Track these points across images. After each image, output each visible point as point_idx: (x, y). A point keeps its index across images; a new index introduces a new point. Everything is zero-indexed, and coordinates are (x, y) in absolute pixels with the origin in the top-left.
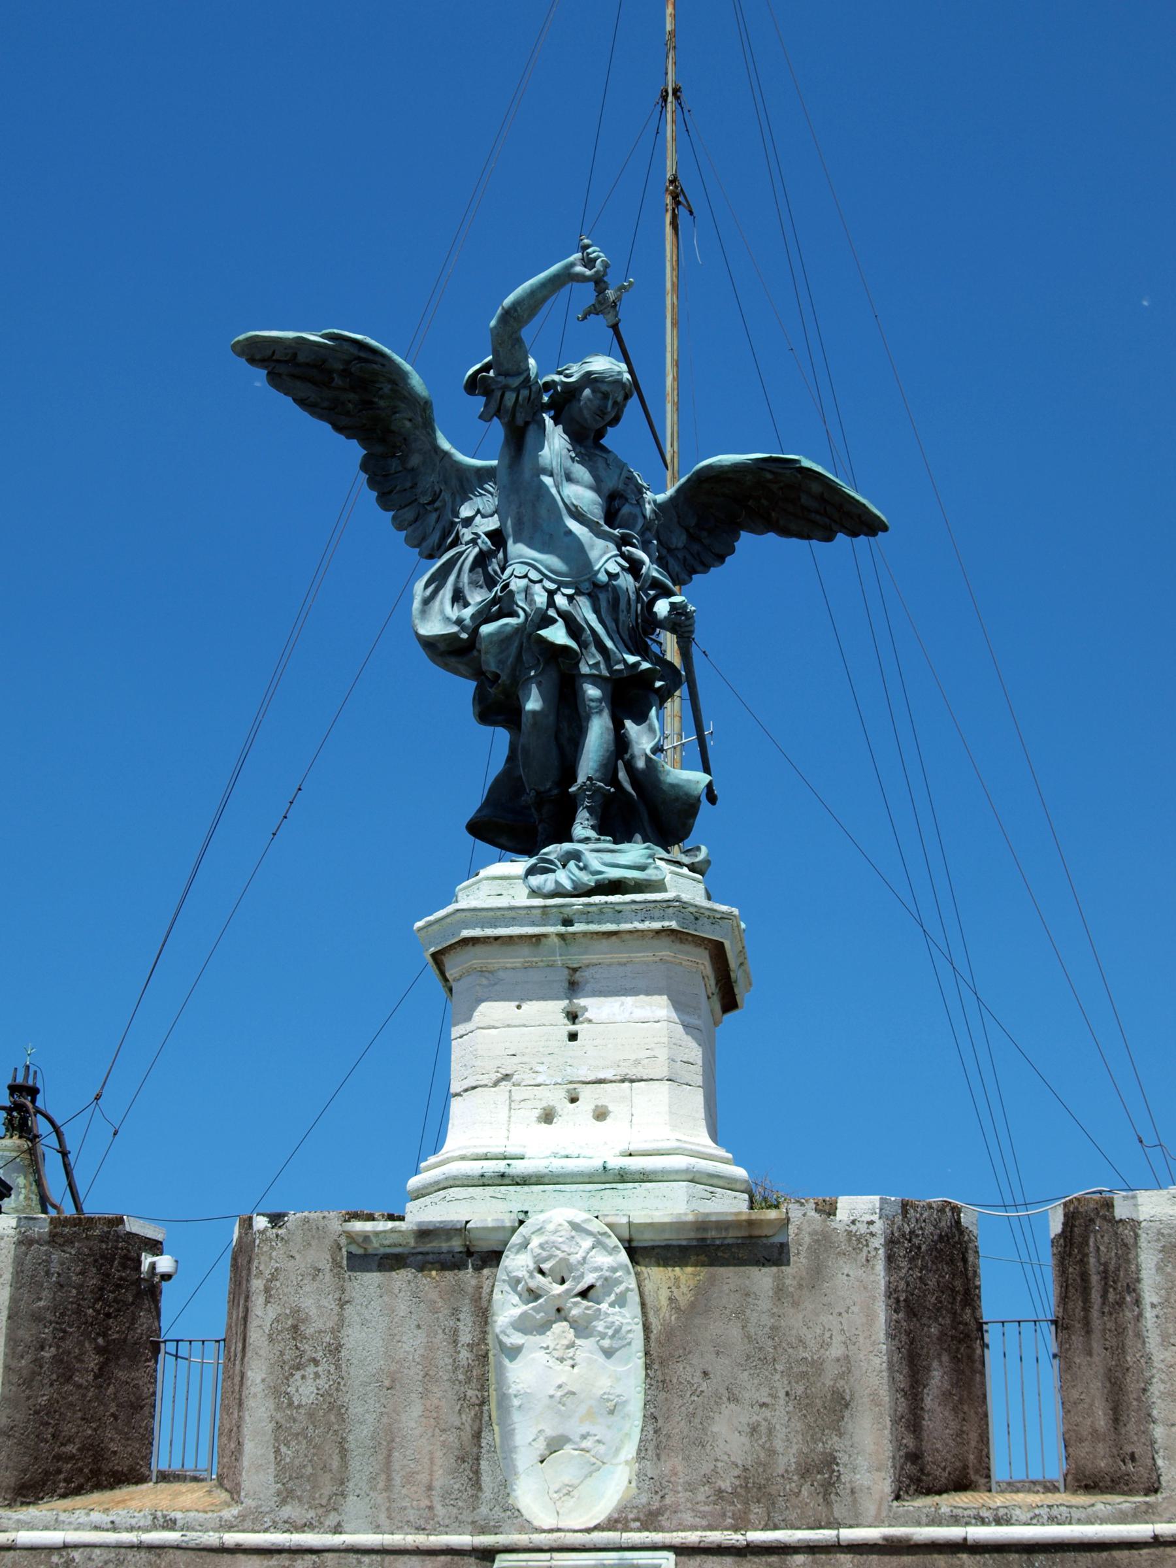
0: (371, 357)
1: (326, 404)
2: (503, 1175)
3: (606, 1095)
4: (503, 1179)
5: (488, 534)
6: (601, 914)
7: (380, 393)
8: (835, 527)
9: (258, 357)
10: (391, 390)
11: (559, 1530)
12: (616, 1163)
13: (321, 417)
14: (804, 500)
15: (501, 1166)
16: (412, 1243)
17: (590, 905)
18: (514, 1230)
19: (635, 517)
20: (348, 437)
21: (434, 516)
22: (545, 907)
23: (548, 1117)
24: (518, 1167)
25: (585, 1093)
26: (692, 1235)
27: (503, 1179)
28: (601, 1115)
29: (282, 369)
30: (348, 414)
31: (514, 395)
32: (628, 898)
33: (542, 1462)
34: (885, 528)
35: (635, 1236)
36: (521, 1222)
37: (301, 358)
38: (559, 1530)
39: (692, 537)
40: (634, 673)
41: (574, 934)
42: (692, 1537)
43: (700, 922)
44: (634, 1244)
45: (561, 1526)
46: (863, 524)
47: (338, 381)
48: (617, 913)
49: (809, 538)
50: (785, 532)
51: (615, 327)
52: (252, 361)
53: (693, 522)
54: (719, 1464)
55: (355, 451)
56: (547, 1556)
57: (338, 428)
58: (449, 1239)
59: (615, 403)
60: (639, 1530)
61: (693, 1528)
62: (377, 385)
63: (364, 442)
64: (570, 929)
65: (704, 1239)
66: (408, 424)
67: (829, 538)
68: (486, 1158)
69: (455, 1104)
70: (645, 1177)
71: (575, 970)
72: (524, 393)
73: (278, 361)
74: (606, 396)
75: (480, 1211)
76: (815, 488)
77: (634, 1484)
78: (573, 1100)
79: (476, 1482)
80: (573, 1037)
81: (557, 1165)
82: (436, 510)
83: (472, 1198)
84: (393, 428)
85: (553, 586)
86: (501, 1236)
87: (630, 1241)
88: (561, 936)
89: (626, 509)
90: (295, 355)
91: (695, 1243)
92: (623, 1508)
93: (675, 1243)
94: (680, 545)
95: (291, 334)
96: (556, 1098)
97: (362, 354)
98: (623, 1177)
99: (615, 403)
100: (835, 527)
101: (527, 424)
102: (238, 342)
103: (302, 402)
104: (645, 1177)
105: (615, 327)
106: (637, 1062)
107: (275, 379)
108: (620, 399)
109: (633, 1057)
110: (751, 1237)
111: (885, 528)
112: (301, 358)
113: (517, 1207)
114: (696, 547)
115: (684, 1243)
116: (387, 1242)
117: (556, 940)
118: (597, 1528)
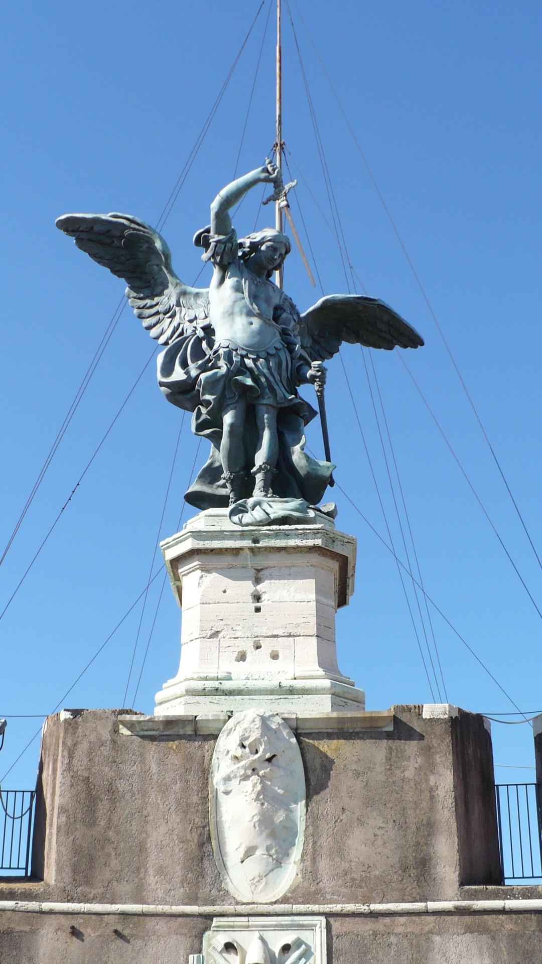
2: (217, 689)
3: (279, 645)
4: (217, 691)
5: (203, 328)
6: (277, 535)
8: (394, 341)
9: (71, 229)
11: (253, 903)
12: (287, 683)
13: (104, 265)
14: (379, 325)
15: (216, 684)
16: (161, 727)
18: (225, 722)
19: (290, 320)
20: (119, 276)
23: (242, 657)
24: (227, 685)
25: (264, 643)
26: (335, 726)
27: (217, 691)
28: (275, 656)
29: (83, 236)
30: (121, 263)
31: (223, 246)
32: (293, 527)
33: (242, 862)
34: (422, 344)
35: (300, 726)
36: (230, 717)
37: (96, 228)
38: (253, 903)
39: (314, 341)
40: (291, 404)
41: (259, 548)
42: (337, 908)
43: (335, 544)
44: (299, 731)
45: (255, 901)
46: (412, 340)
48: (287, 535)
49: (380, 348)
50: (367, 343)
52: (67, 230)
53: (316, 333)
54: (353, 864)
56: (246, 919)
57: (114, 271)
58: (184, 727)
59: (281, 255)
60: (303, 903)
61: (337, 902)
64: (257, 545)
65: (342, 729)
66: (156, 268)
67: (390, 348)
68: (206, 679)
69: (183, 648)
70: (305, 692)
71: (258, 571)
72: (229, 245)
73: (82, 231)
75: (205, 710)
76: (386, 318)
77: (300, 876)
78: (258, 647)
79: (202, 874)
80: (258, 610)
81: (251, 684)
82: (169, 317)
83: (198, 703)
84: (147, 270)
85: (244, 353)
86: (217, 725)
87: (296, 729)
88: (251, 549)
89: (284, 315)
90: (92, 228)
91: (336, 731)
92: (294, 890)
93: (325, 731)
94: (309, 345)
95: (89, 216)
96: (247, 646)
98: (291, 691)
99: (281, 255)
100: (394, 341)
101: (229, 264)
102: (60, 221)
103: (93, 255)
104: (305, 692)
106: (298, 625)
107: (81, 243)
108: (283, 252)
109: (295, 622)
110: (371, 727)
111: (422, 344)
112: (96, 228)
113: (226, 708)
114: (317, 347)
115: (330, 731)
116: (145, 728)
117: (248, 552)
118: (275, 903)
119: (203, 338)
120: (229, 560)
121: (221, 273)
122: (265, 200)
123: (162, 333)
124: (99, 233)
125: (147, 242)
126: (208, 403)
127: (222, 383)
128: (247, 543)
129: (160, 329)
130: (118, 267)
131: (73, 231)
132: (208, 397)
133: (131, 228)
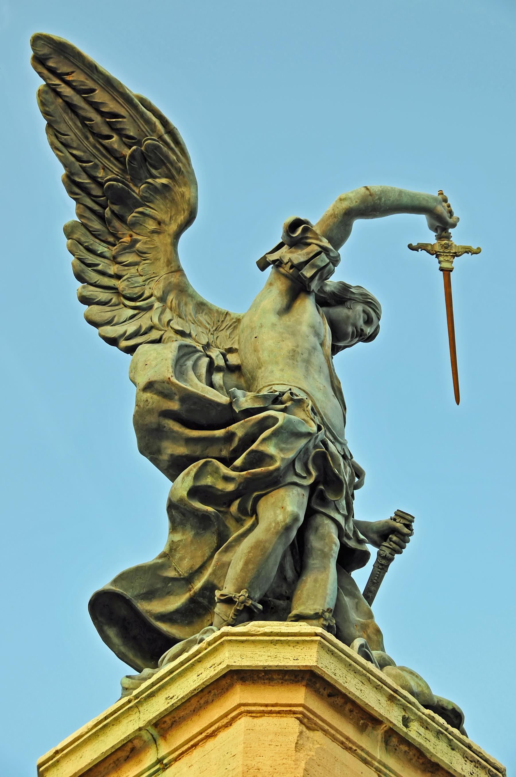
0: (172, 145)
1: (75, 152)
7: (150, 180)
9: (51, 64)
10: (164, 185)
17: (433, 719)
21: (131, 312)
22: (395, 691)
29: (66, 91)
40: (359, 547)
47: (115, 141)
51: (447, 272)
55: (69, 210)
62: (154, 171)
63: (84, 210)
66: (151, 225)
74: (369, 321)
97: (166, 137)
105: (447, 272)
107: (49, 97)
119: (219, 369)
120: (348, 730)
121: (285, 302)
122: (414, 244)
123: (109, 323)
124: (96, 106)
125: (170, 176)
126: (260, 458)
127: (302, 443)
128: (394, 716)
129: (108, 316)
130: (84, 180)
131: (52, 71)
132: (271, 449)
133: (161, 138)
